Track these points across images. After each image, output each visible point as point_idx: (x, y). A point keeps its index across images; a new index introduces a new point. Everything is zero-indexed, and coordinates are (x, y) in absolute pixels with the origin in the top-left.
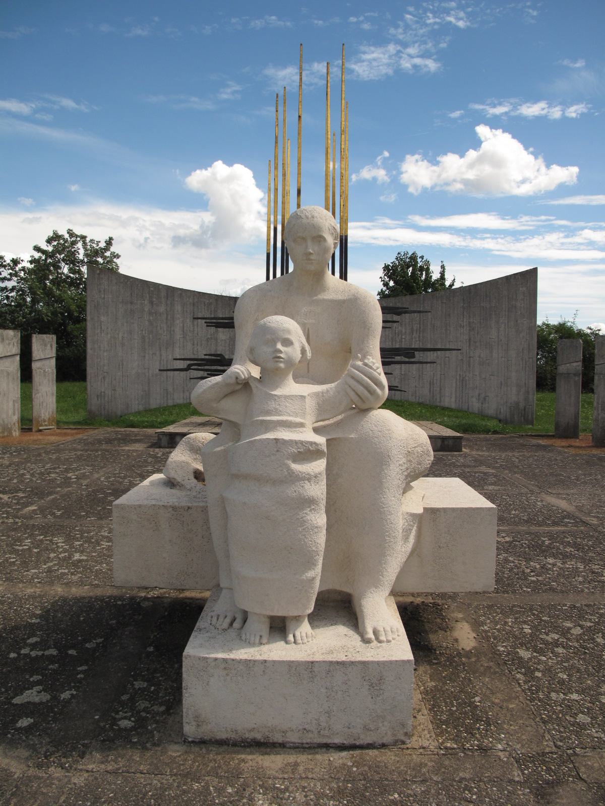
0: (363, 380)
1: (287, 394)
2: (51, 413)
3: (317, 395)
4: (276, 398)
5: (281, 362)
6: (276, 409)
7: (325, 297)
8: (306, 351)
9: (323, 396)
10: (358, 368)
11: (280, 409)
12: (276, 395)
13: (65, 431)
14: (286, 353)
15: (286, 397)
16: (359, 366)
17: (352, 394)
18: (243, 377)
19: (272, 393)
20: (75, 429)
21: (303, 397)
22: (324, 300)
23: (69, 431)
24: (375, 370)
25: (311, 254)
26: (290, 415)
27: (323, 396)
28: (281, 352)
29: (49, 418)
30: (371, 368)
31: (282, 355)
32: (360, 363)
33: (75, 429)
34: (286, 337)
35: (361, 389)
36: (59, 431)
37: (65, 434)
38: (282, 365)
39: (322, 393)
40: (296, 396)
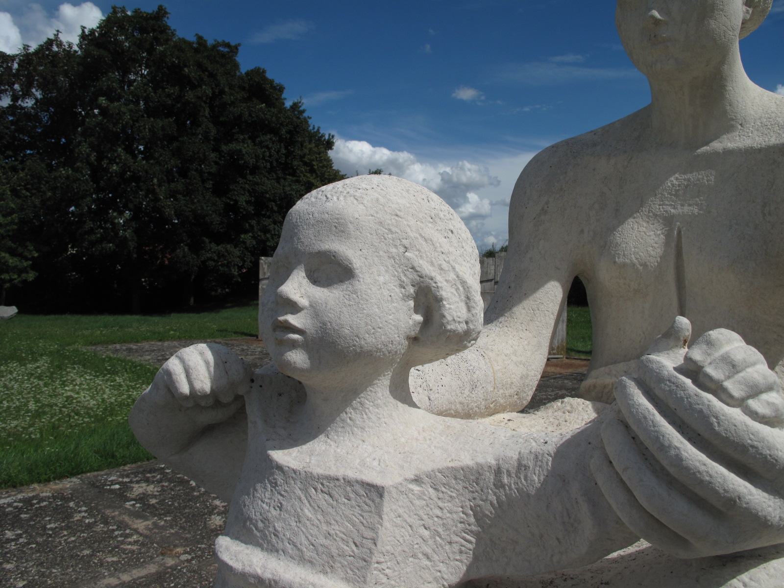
0: (664, 447)
1: (318, 470)
2: (560, 341)
3: (470, 477)
4: (280, 479)
5: (294, 345)
6: (265, 520)
7: (730, 145)
8: (439, 300)
9: (499, 485)
10: (652, 385)
11: (278, 526)
12: (280, 468)
13: (574, 361)
14: (315, 310)
15: (310, 481)
16: (660, 378)
17: (614, 500)
18: (185, 389)
19: (278, 456)
20: (585, 360)
21: (375, 492)
22: (728, 153)
23: (578, 362)
24: (740, 403)
25: (657, 22)
26: (302, 560)
27: (499, 485)
28: (294, 308)
29: (558, 346)
30: (718, 390)
31: (293, 320)
32: (668, 361)
33: (585, 360)
34: (327, 247)
35: (645, 487)
36: (567, 361)
37: (571, 366)
38: (298, 358)
39: (498, 471)
40: (349, 482)
